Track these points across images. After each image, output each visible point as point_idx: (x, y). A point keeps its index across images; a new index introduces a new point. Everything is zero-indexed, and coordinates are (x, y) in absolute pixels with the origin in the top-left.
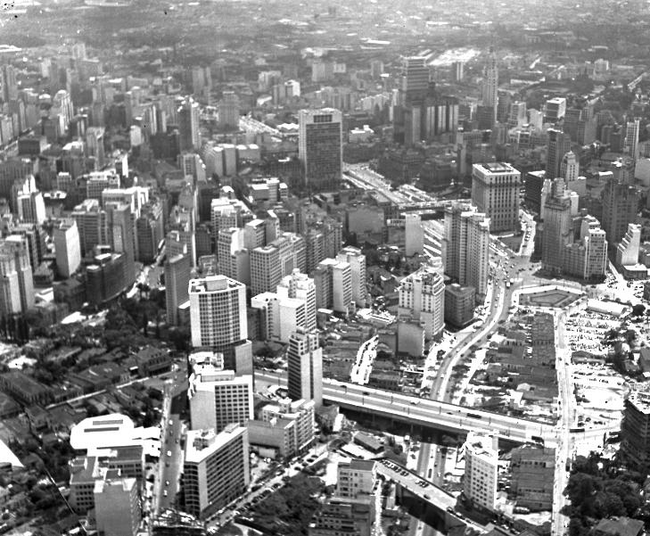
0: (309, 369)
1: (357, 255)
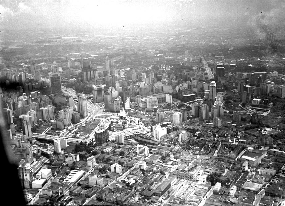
0: (27, 129)
1: (50, 106)
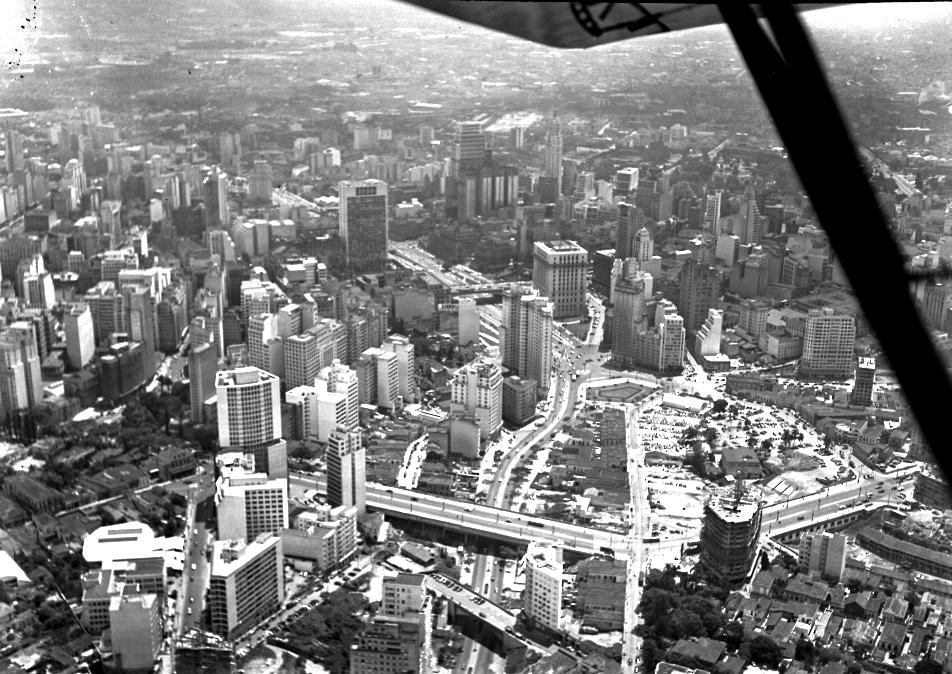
0: (350, 472)
1: (404, 344)
